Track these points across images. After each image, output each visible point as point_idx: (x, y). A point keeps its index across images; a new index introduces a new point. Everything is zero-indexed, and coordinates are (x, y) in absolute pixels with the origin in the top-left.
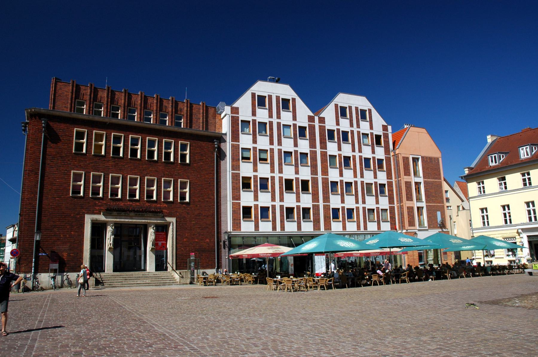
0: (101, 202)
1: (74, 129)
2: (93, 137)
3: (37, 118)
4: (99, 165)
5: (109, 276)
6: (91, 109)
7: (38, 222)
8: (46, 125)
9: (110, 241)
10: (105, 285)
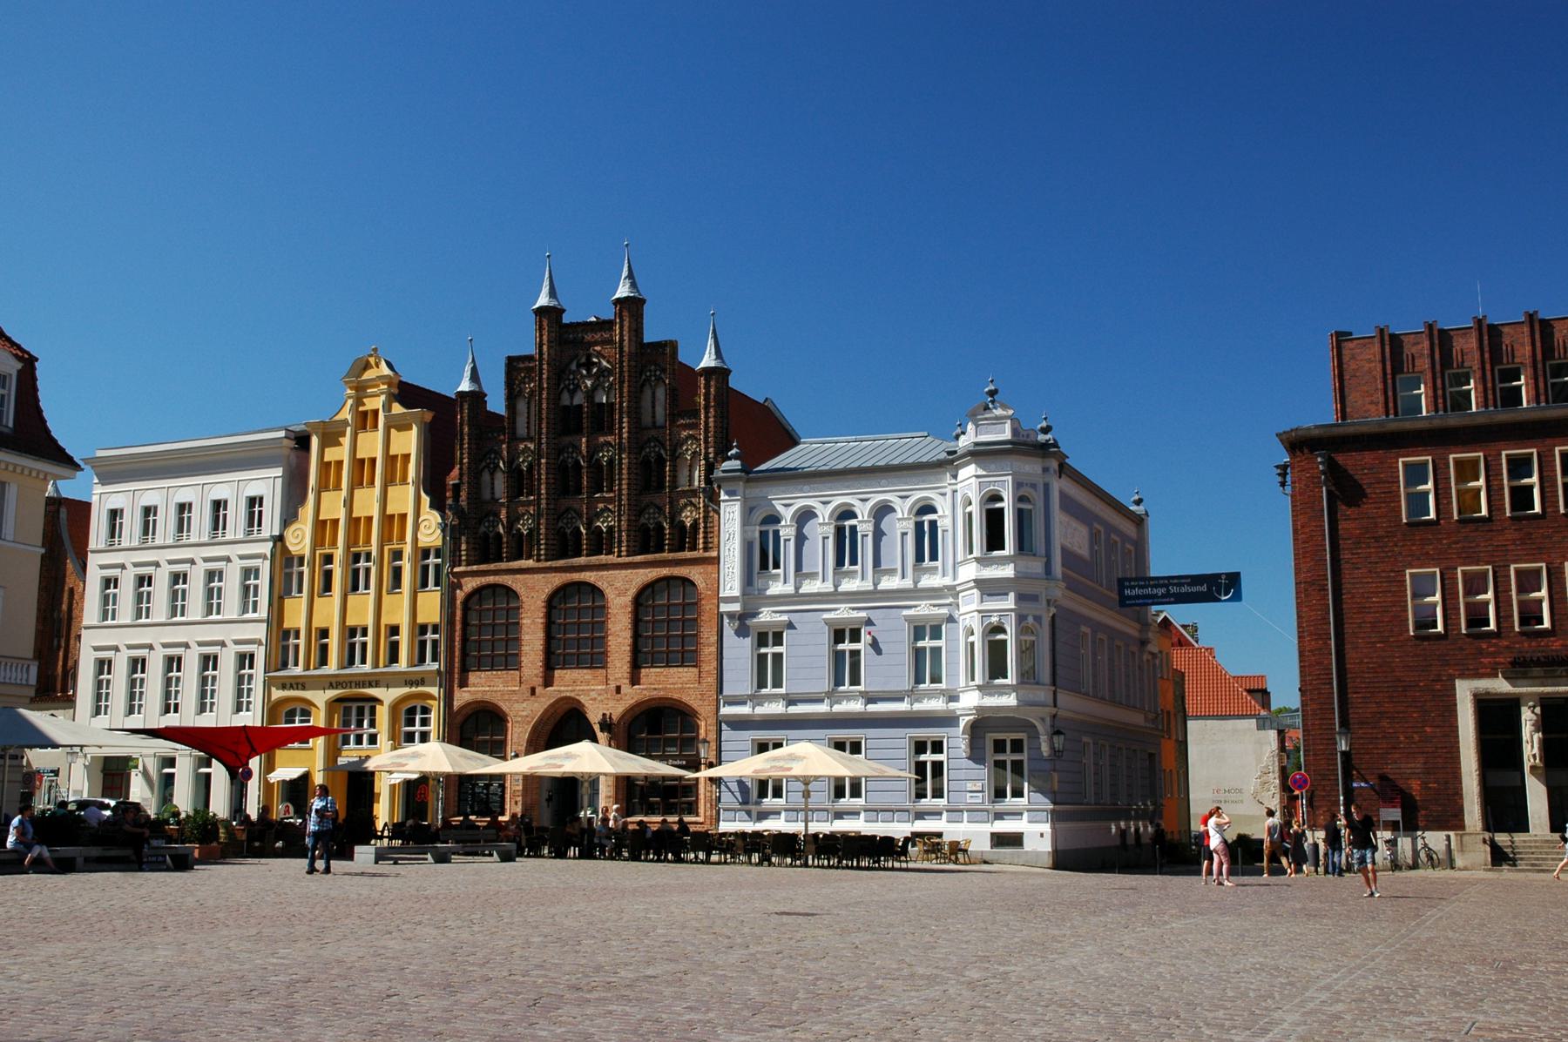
0: (1495, 645)
1: (1398, 462)
2: (1449, 472)
3: (1306, 451)
4: (1478, 546)
5: (1536, 841)
6: (1440, 392)
7: (1340, 707)
8: (1328, 467)
9: (1532, 747)
10: (1520, 865)
